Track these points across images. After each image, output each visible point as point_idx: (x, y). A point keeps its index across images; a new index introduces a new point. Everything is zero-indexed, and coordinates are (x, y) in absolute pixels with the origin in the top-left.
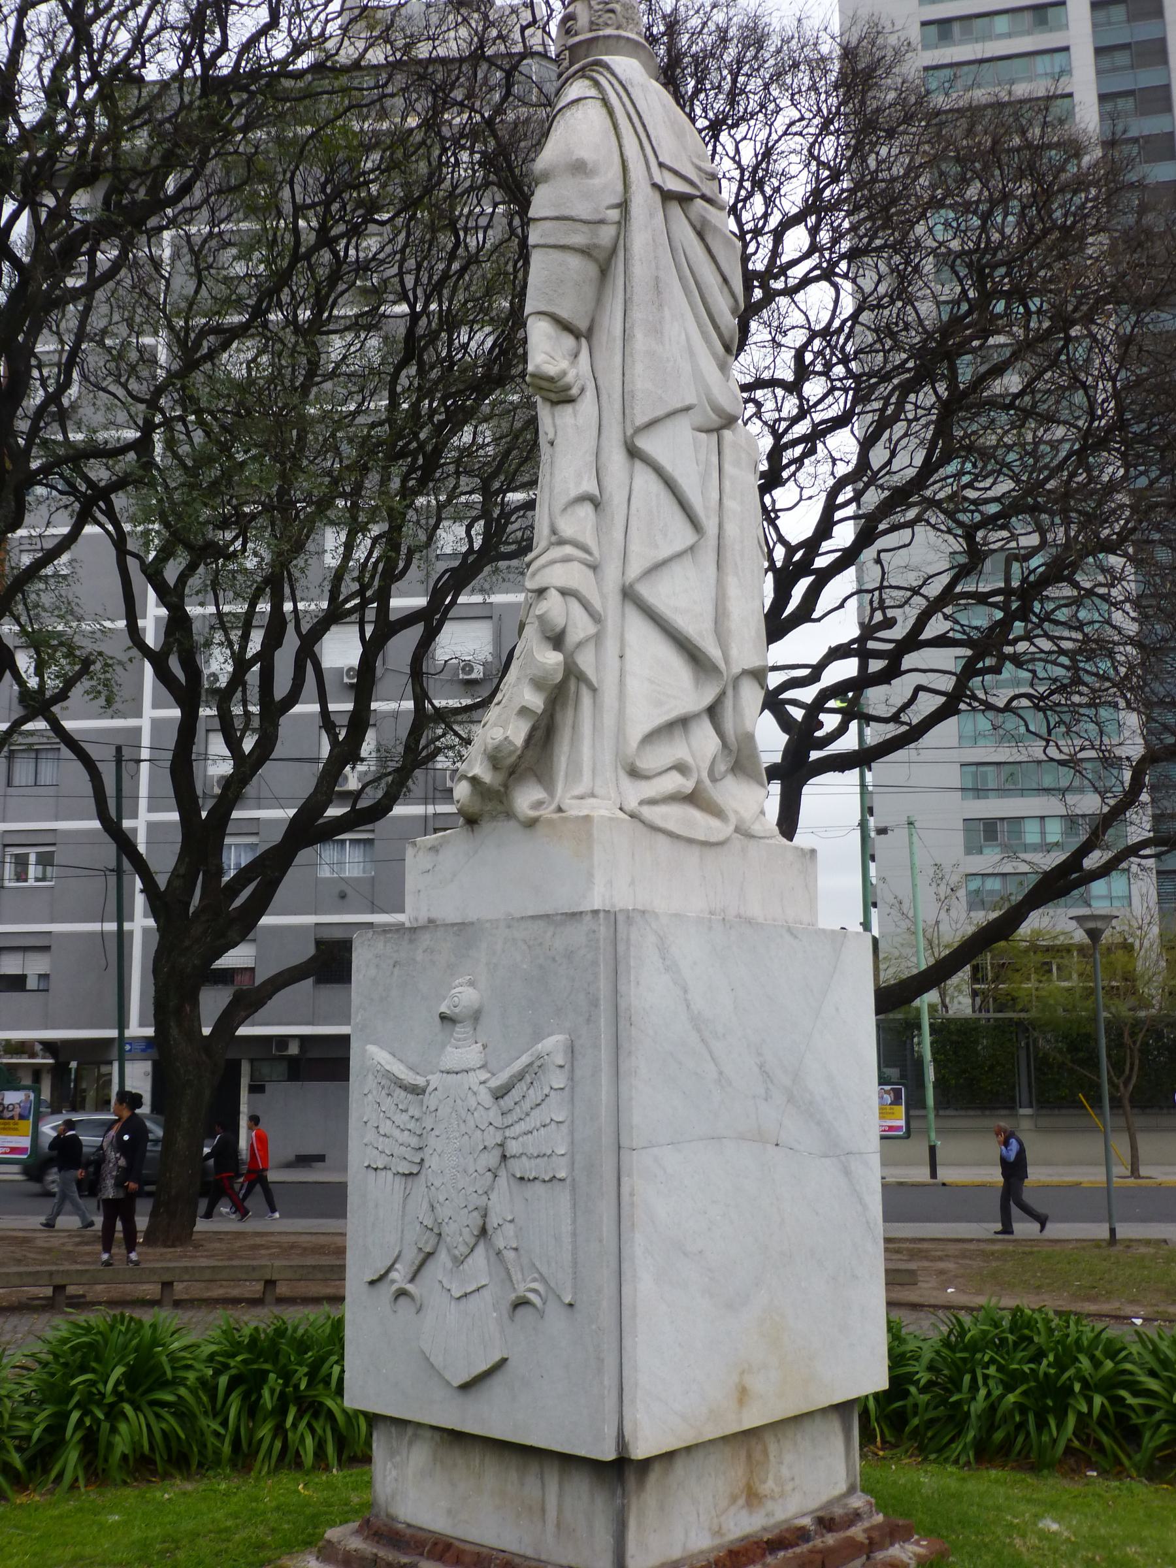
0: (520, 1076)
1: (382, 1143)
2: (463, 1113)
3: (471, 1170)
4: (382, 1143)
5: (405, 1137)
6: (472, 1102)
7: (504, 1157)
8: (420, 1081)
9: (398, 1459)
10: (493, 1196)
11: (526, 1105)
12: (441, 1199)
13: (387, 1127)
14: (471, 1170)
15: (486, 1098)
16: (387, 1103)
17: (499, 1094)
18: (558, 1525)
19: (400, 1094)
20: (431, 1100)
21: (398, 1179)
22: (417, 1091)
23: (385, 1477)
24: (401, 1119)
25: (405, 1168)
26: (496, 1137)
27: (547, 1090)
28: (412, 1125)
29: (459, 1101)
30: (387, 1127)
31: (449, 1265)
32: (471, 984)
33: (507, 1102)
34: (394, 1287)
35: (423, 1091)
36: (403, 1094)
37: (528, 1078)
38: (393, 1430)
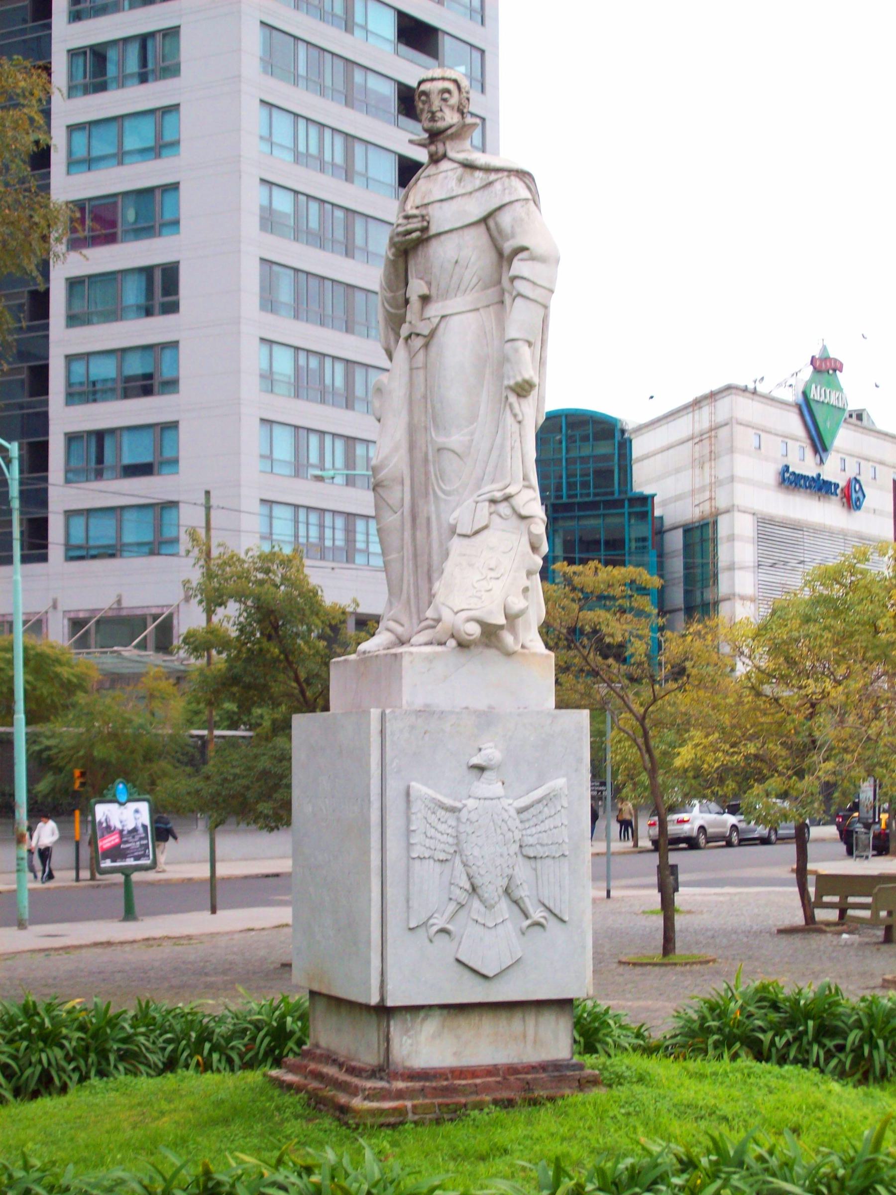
0: (539, 801)
1: (428, 842)
2: (500, 822)
3: (505, 854)
4: (428, 842)
5: (444, 838)
6: (506, 817)
7: (521, 846)
8: (458, 805)
9: (412, 1032)
10: (516, 868)
11: (541, 817)
12: (482, 872)
13: (431, 832)
14: (505, 854)
15: (513, 813)
16: (432, 819)
17: (520, 811)
18: (535, 1042)
19: (441, 813)
20: (464, 814)
21: (438, 864)
22: (453, 810)
23: (401, 1046)
24: (442, 827)
25: (442, 856)
26: (518, 835)
27: (559, 808)
28: (450, 831)
29: (495, 816)
30: (431, 832)
31: (483, 909)
32: (496, 747)
33: (524, 816)
34: (435, 928)
35: (460, 810)
36: (443, 812)
37: (545, 802)
38: (408, 1016)
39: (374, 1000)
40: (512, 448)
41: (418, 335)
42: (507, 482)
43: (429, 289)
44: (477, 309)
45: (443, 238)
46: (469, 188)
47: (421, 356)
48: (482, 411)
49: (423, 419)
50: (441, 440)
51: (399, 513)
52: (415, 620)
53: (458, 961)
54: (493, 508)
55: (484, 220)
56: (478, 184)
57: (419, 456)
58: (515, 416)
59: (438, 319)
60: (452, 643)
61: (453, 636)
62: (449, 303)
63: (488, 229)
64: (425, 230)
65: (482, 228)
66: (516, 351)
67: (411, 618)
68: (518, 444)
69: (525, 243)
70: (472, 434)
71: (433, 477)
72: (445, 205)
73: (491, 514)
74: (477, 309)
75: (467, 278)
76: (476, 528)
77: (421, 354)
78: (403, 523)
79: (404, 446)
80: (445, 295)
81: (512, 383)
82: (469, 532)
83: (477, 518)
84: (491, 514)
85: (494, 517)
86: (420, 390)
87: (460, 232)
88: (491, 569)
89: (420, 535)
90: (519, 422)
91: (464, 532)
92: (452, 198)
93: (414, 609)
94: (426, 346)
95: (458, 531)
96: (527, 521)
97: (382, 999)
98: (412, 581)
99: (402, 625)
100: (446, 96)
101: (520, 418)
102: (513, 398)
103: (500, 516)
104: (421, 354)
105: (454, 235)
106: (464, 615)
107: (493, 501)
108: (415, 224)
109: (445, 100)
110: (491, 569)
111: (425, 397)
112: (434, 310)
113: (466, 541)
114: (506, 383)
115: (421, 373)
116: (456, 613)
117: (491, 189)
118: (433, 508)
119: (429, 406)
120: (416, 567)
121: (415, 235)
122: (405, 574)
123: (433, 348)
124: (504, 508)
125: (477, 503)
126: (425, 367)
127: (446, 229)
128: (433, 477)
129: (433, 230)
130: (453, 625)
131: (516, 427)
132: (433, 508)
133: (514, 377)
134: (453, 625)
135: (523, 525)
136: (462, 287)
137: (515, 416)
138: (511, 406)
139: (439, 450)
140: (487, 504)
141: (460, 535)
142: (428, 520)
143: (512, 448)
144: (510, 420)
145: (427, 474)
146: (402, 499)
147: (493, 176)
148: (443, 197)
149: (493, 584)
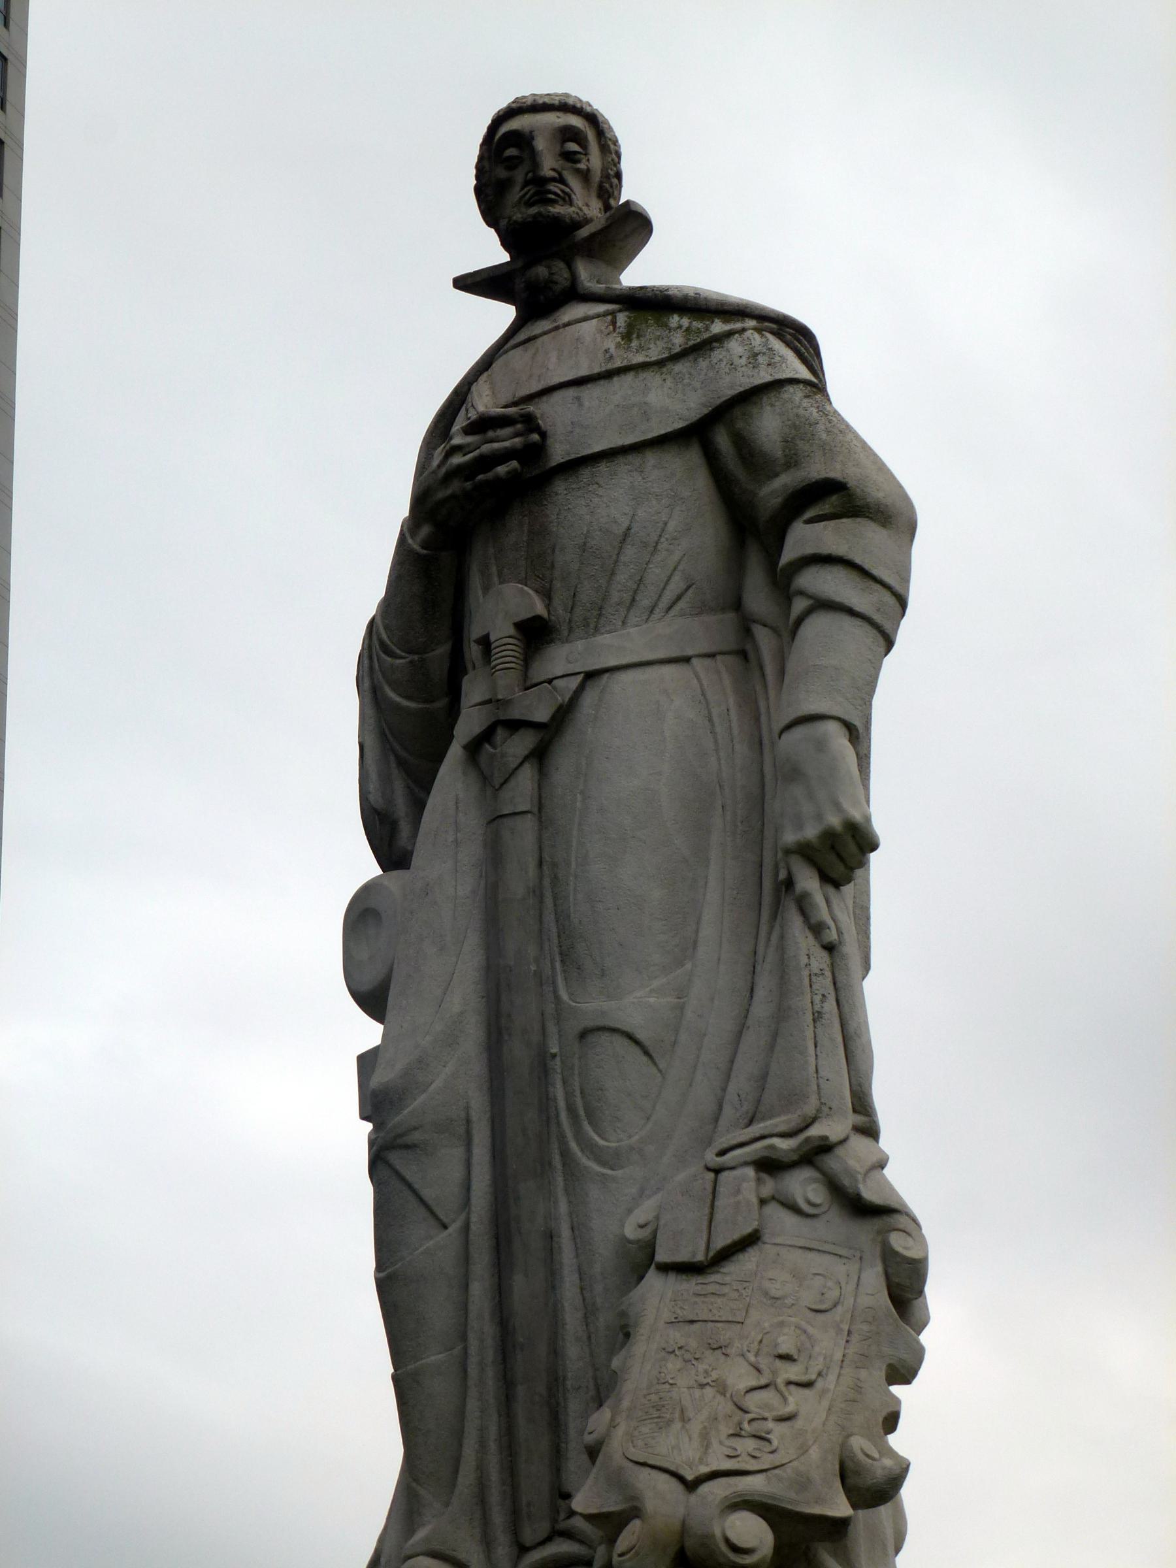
40: (817, 1017)
41: (515, 726)
42: (810, 1108)
43: (548, 606)
44: (686, 660)
45: (586, 473)
46: (655, 353)
48: (708, 931)
49: (532, 951)
54: (769, 1186)
56: (678, 341)
57: (518, 1052)
58: (817, 929)
59: (574, 683)
62: (604, 639)
63: (712, 458)
64: (534, 452)
65: (693, 456)
66: (821, 745)
68: (830, 1006)
69: (835, 473)
70: (682, 992)
71: (563, 1116)
72: (591, 394)
73: (763, 1202)
74: (686, 660)
75: (655, 574)
76: (721, 1241)
77: (526, 778)
78: (466, 1258)
79: (473, 1033)
80: (594, 623)
81: (811, 832)
82: (700, 1257)
83: (719, 1216)
84: (763, 1202)
85: (773, 1210)
87: (634, 459)
88: (786, 1358)
89: (521, 1286)
90: (830, 948)
91: (683, 1256)
92: (608, 375)
93: (499, 1518)
94: (540, 755)
95: (661, 1256)
96: (878, 1223)
98: (493, 1431)
100: (573, 147)
101: (832, 935)
102: (808, 881)
104: (526, 778)
106: (717, 1490)
107: (769, 1166)
108: (506, 440)
109: (569, 157)
110: (786, 1358)
111: (537, 892)
113: (689, 1285)
114: (790, 837)
115: (527, 825)
116: (691, 1486)
117: (718, 354)
118: (563, 1207)
119: (549, 918)
120: (507, 1383)
122: (472, 1405)
123: (564, 762)
125: (717, 1171)
126: (540, 809)
127: (597, 448)
128: (563, 1116)
129: (559, 453)
130: (684, 1529)
131: (820, 960)
132: (563, 1207)
133: (819, 817)
134: (684, 1529)
135: (864, 1232)
136: (644, 602)
137: (817, 929)
138: (803, 905)
139: (584, 1035)
140: (750, 1172)
141: (665, 1268)
142: (550, 1236)
143: (817, 1017)
144: (802, 942)
145: (546, 1104)
146: (467, 1186)
147: (718, 327)
148: (583, 372)
149: (796, 1400)
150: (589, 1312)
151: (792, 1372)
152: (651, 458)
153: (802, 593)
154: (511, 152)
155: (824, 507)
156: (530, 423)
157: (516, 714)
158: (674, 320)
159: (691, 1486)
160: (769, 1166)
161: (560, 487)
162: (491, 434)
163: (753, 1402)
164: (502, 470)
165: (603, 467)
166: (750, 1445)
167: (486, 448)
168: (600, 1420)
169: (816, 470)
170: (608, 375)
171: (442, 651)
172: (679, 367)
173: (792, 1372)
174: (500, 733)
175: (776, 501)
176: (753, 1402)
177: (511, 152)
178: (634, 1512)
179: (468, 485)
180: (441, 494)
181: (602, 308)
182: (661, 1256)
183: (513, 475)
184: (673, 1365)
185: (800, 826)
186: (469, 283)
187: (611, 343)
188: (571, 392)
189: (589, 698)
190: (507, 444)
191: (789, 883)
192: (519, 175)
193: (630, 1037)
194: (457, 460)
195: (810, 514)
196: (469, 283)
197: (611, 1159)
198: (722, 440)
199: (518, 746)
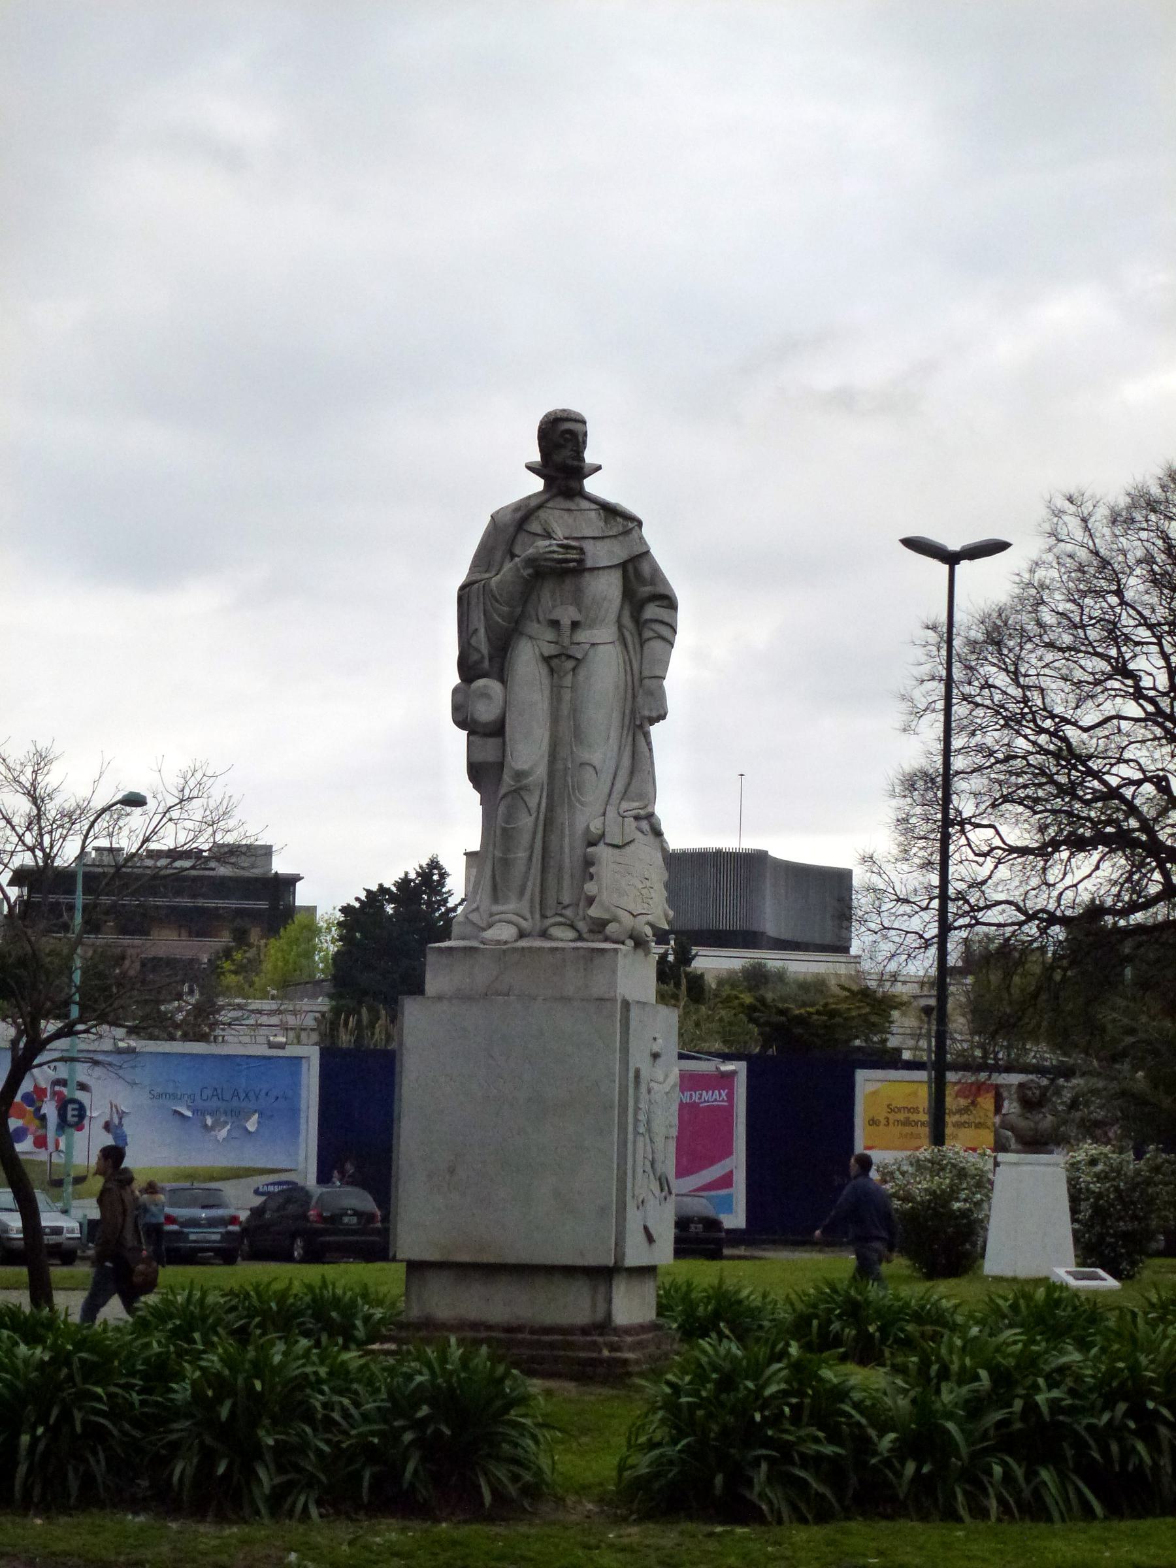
39: (611, 1263)
41: (569, 657)
47: (570, 677)
50: (586, 756)
51: (534, 815)
52: (537, 916)
53: (646, 1229)
55: (624, 566)
56: (621, 529)
60: (630, 943)
61: (631, 937)
62: (595, 631)
64: (581, 561)
67: (532, 913)
72: (599, 543)
86: (565, 709)
92: (603, 538)
94: (574, 669)
97: (615, 1263)
99: (525, 919)
103: (643, 832)
105: (606, 572)
107: (637, 818)
112: (582, 636)
113: (616, 851)
121: (572, 565)
123: (582, 672)
124: (645, 825)
126: (573, 688)
129: (589, 564)
130: (633, 929)
133: (658, 710)
134: (633, 929)
135: (658, 840)
139: (582, 764)
150: (572, 849)
151: (648, 884)
152: (613, 570)
153: (653, 630)
154: (568, 436)
155: (665, 603)
156: (581, 551)
157: (571, 654)
158: (619, 519)
159: (634, 916)
160: (637, 818)
161: (587, 574)
162: (569, 551)
163: (643, 891)
164: (572, 565)
165: (601, 572)
166: (646, 906)
167: (569, 556)
168: (590, 888)
169: (661, 590)
170: (603, 538)
171: (519, 610)
172: (621, 538)
173: (648, 884)
174: (563, 658)
175: (646, 595)
176: (643, 891)
177: (568, 436)
178: (615, 919)
179: (558, 565)
180: (542, 563)
181: (595, 507)
182: (608, 840)
183: (574, 567)
184: (618, 876)
185: (651, 710)
186: (530, 468)
187: (602, 524)
188: (591, 541)
189: (591, 653)
190: (574, 556)
191: (641, 726)
192: (570, 445)
193: (594, 767)
194: (556, 556)
195: (657, 603)
196: (530, 468)
197: (582, 804)
198: (630, 568)
199: (570, 664)
